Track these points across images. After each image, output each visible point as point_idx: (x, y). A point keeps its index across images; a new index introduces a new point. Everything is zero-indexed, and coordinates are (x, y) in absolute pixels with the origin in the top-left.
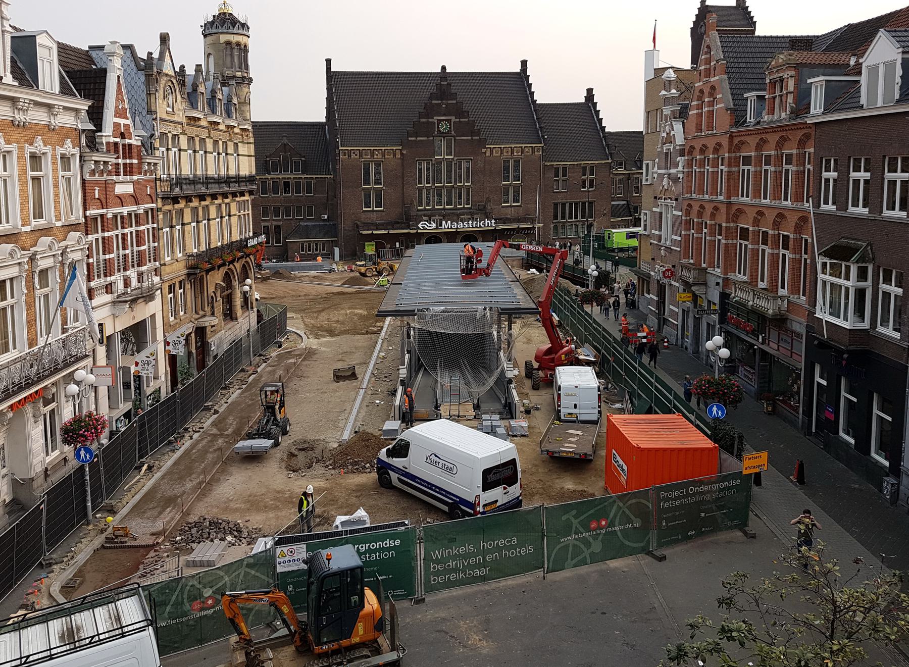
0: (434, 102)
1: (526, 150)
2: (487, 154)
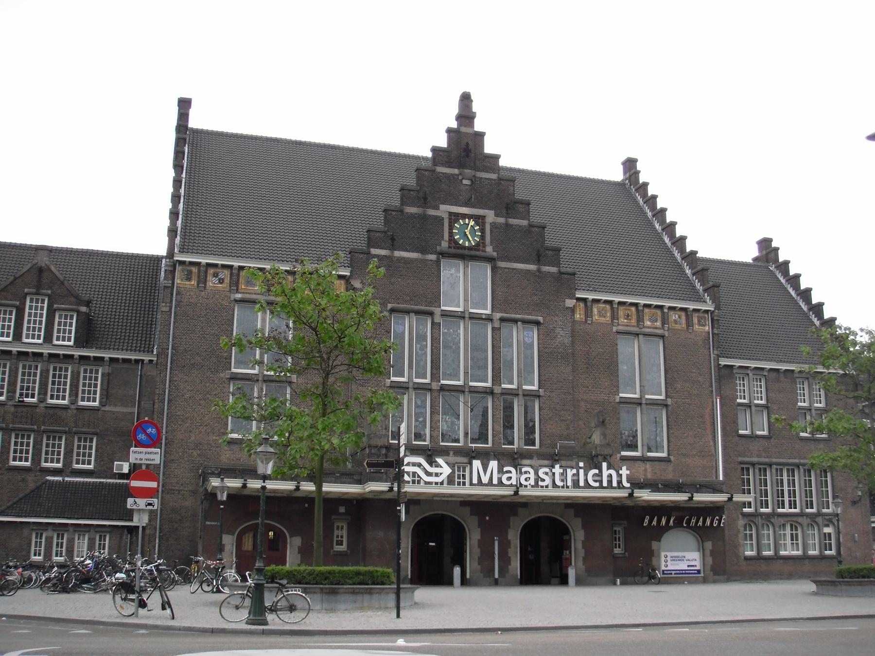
0: (441, 169)
1: (674, 316)
2: (577, 316)
